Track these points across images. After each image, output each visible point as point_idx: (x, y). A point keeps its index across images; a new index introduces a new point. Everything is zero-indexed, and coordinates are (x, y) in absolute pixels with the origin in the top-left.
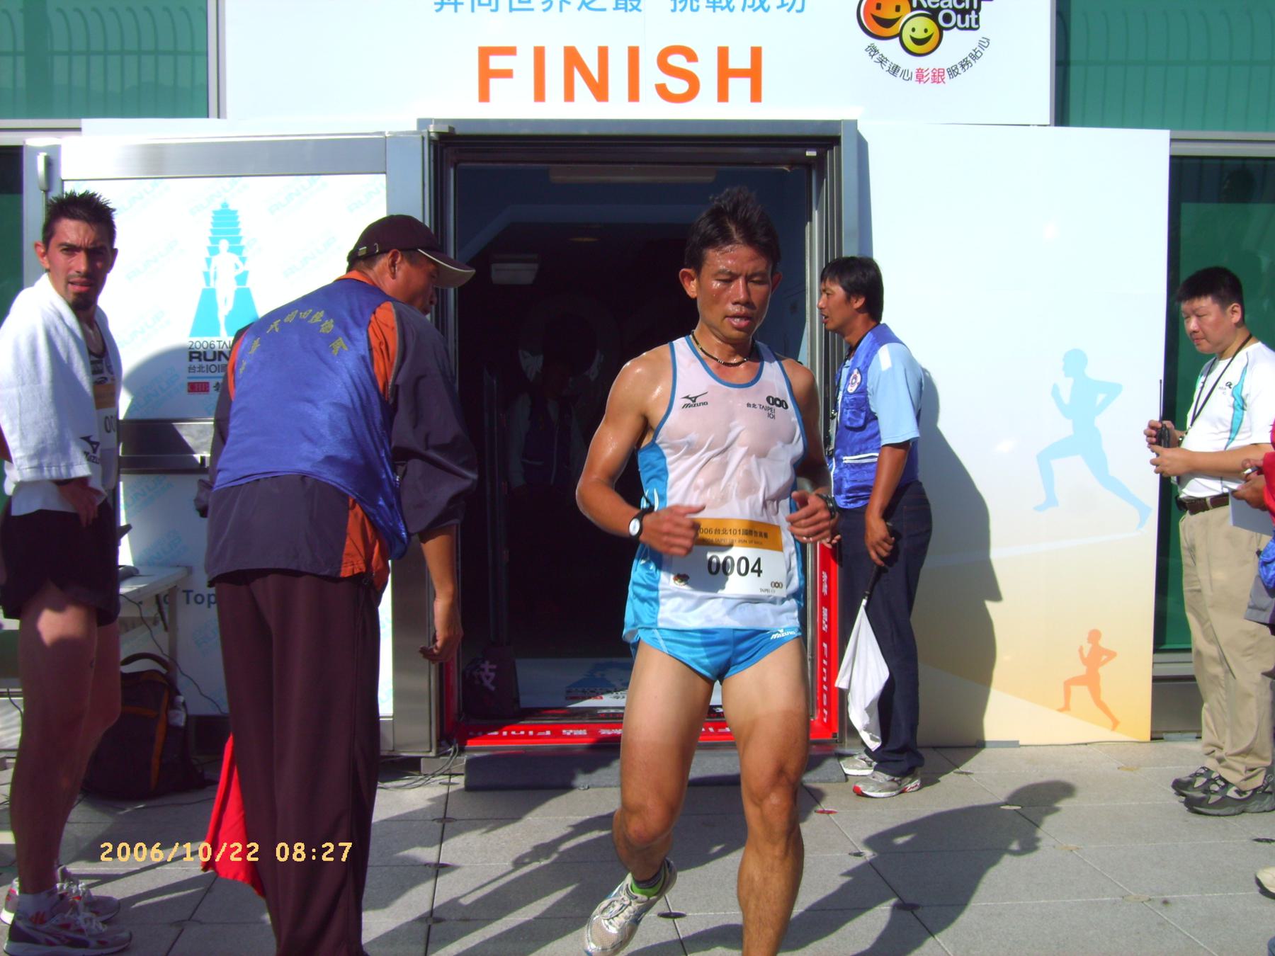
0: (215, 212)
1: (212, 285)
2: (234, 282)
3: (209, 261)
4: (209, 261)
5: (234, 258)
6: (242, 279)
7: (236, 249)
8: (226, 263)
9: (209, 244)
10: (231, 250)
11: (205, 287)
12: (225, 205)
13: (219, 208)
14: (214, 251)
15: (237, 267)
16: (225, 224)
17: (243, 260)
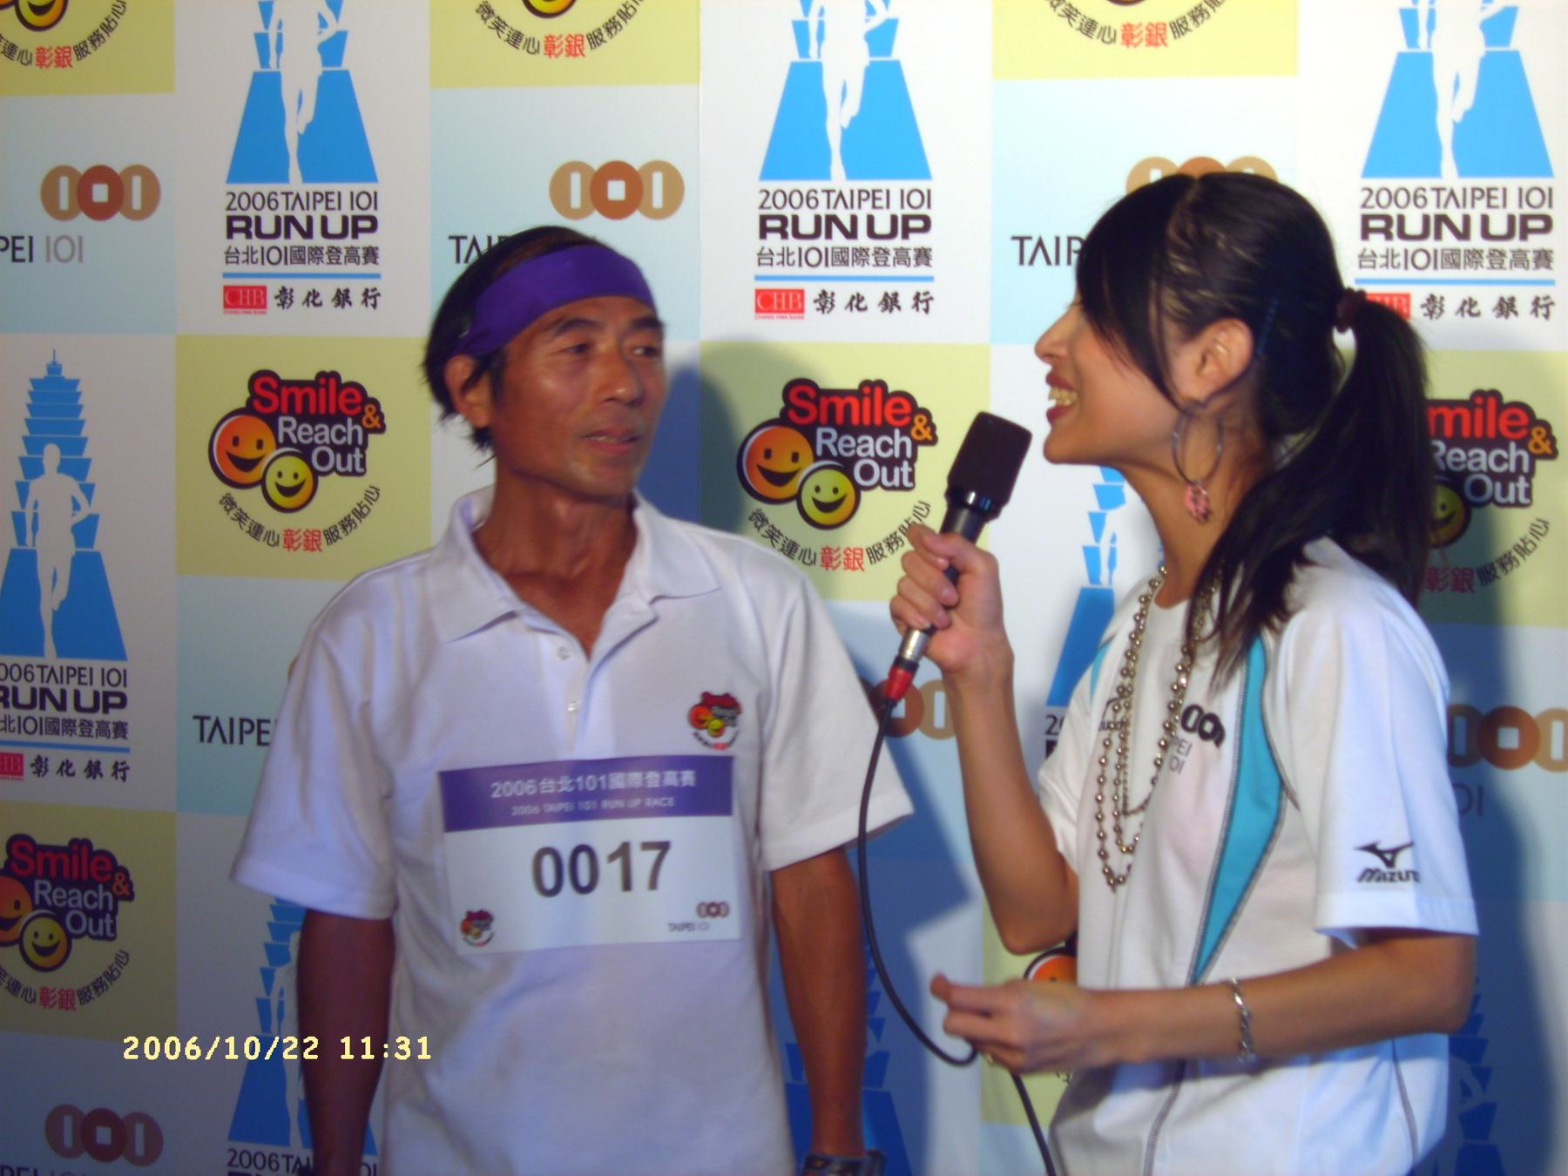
0: (34, 382)
1: (29, 545)
2: (71, 538)
3: (23, 490)
4: (23, 490)
5: (70, 485)
6: (85, 531)
7: (76, 467)
9: (24, 453)
10: (64, 468)
11: (15, 545)
12: (54, 368)
13: (41, 373)
14: (32, 468)
15: (76, 506)
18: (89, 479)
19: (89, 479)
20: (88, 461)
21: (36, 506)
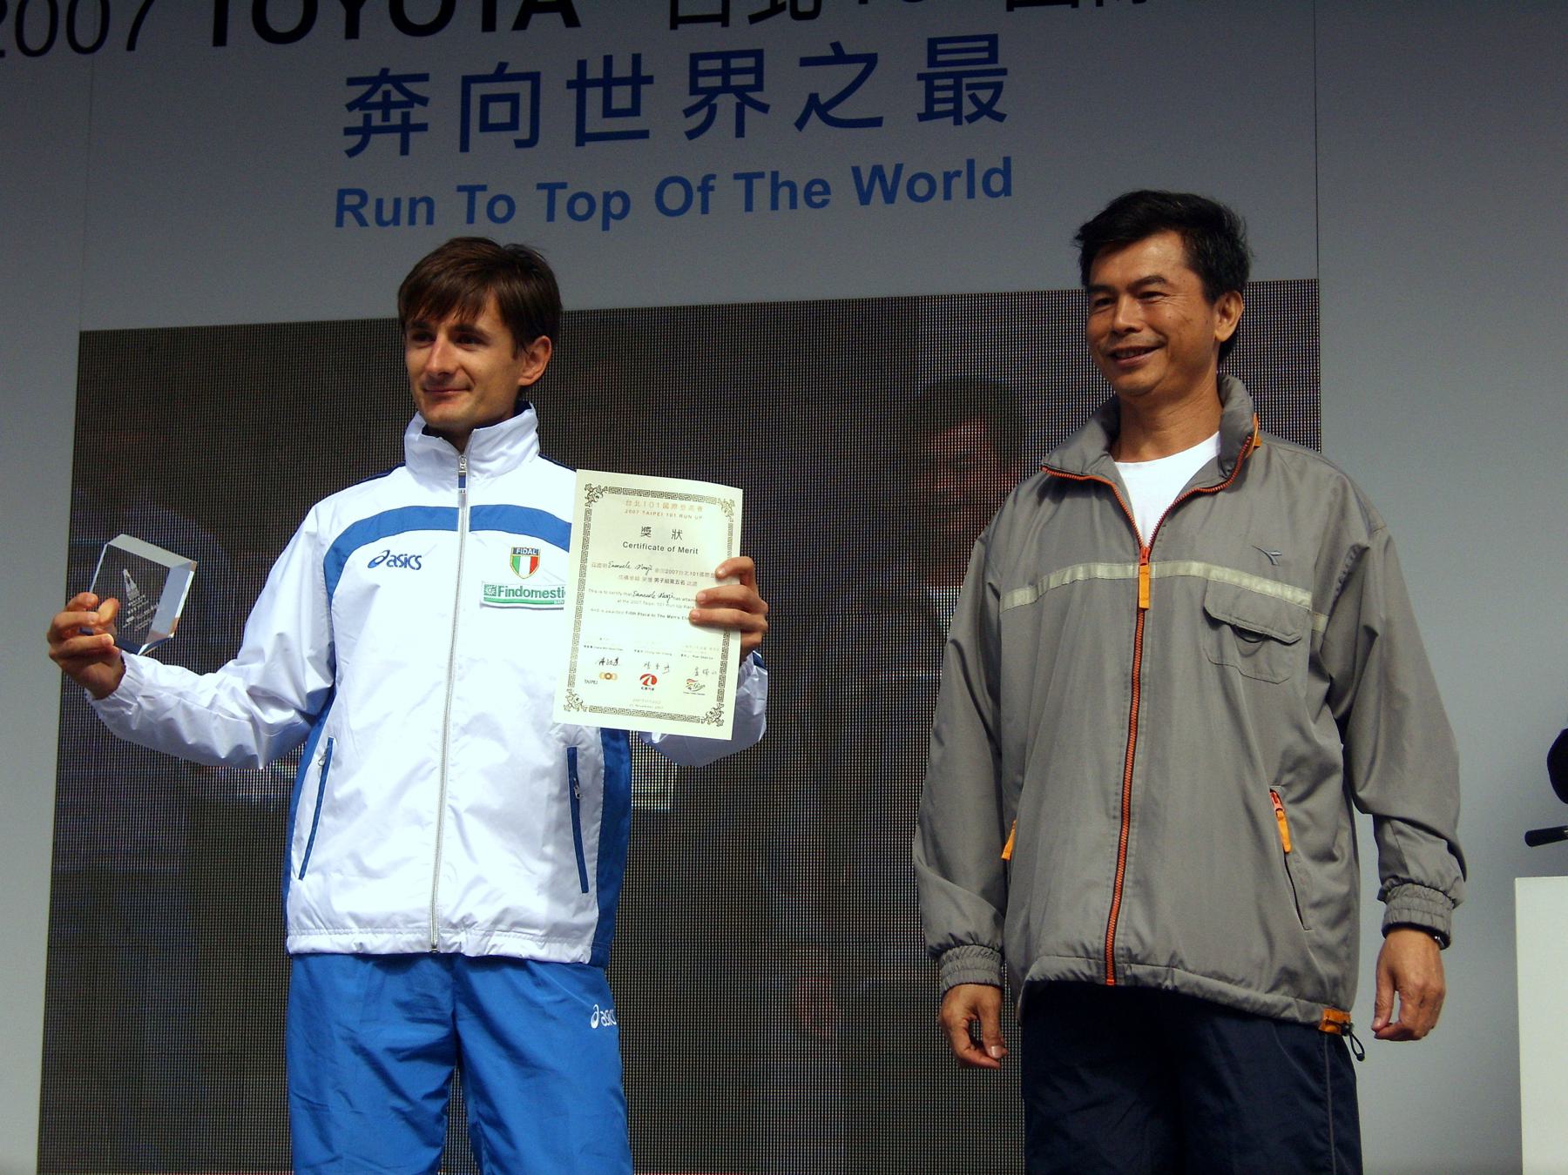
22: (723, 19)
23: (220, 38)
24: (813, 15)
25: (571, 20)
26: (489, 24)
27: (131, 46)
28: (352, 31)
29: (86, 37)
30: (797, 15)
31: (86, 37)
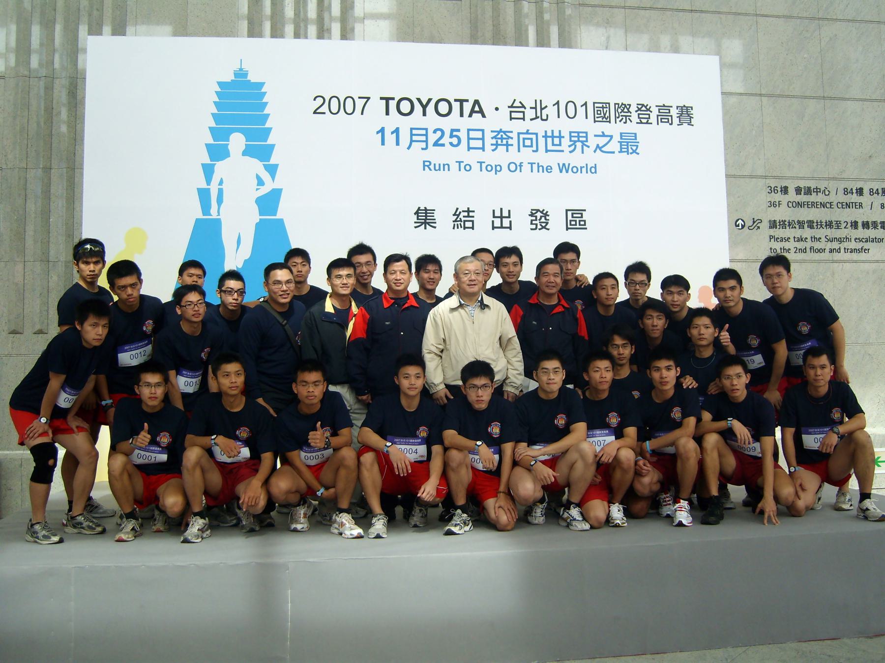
0: (220, 84)
3: (208, 171)
4: (208, 171)
5: (256, 166)
6: (268, 203)
7: (260, 149)
8: (239, 173)
10: (248, 152)
11: (201, 216)
12: (241, 74)
13: (229, 77)
14: (218, 152)
15: (260, 182)
16: (241, 108)
17: (272, 170)
18: (273, 161)
19: (273, 161)
20: (272, 147)
21: (221, 183)
22: (523, 119)
23: (387, 113)
24: (546, 120)
25: (484, 116)
26: (462, 115)
27: (362, 114)
28: (424, 114)
29: (349, 109)
30: (542, 120)
31: (349, 109)
